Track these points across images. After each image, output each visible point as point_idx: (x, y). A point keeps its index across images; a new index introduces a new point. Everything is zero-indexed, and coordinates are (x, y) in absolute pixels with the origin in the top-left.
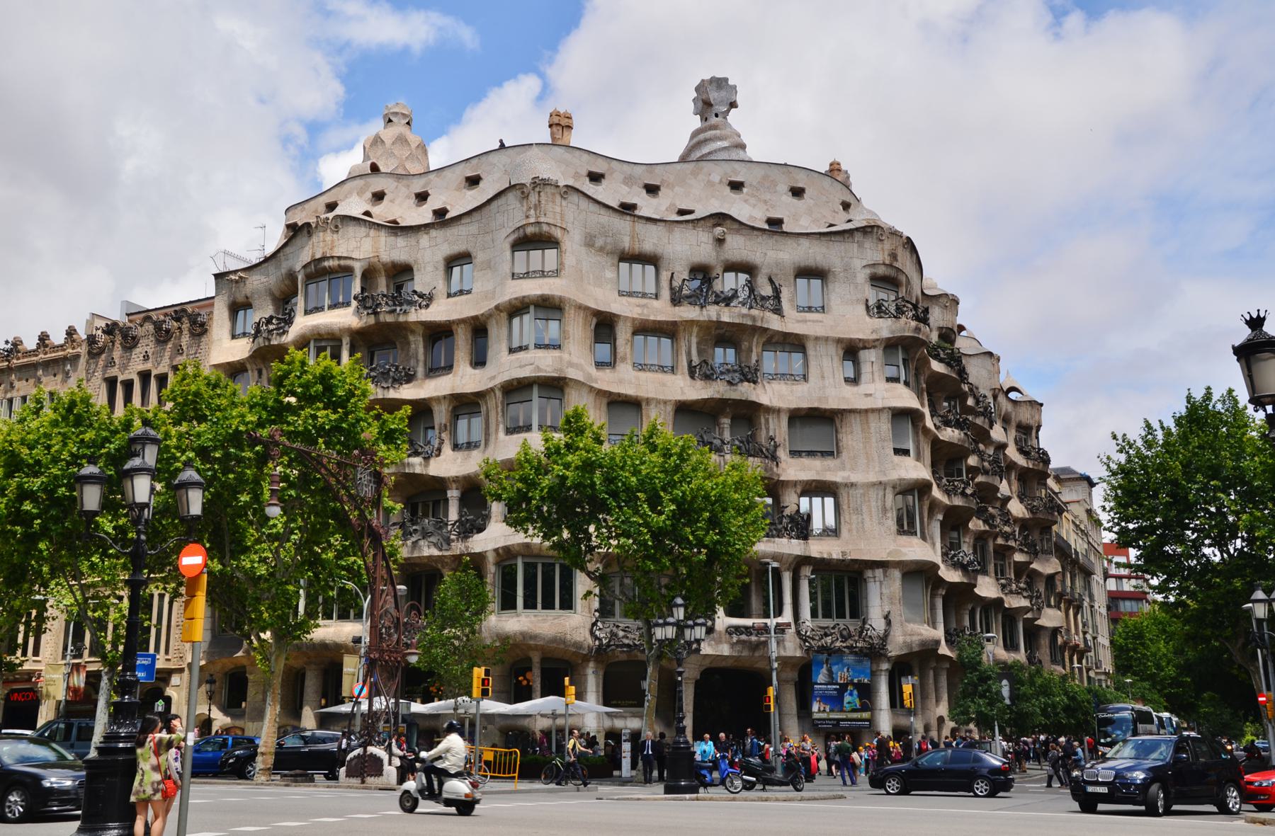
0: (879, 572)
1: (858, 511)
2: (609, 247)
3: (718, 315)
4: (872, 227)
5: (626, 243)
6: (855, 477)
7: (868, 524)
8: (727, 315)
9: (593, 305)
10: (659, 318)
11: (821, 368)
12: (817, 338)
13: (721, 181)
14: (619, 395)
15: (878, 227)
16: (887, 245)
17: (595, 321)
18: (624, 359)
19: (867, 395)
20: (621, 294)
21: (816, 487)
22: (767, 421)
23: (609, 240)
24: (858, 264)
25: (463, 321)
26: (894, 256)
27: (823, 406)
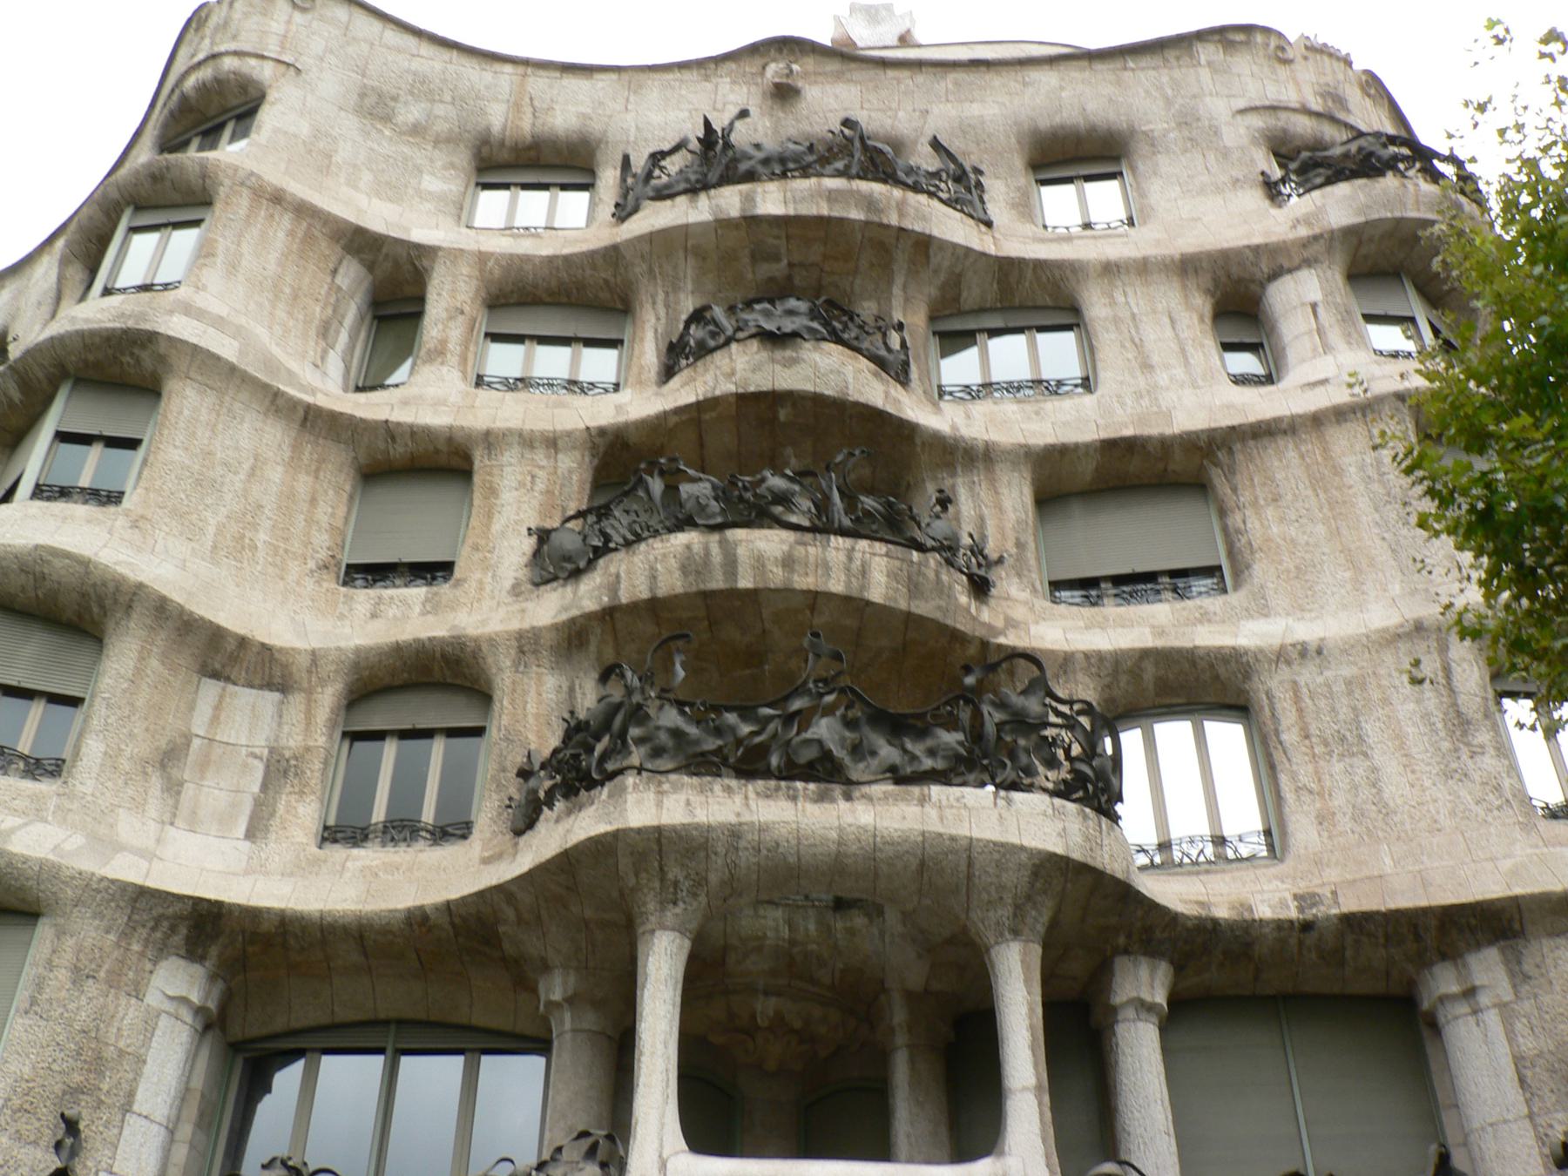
1: (1351, 744)
2: (441, 127)
3: (749, 199)
4: (1248, 29)
5: (496, 118)
6: (1306, 631)
7: (1396, 786)
10: (566, 251)
11: (1139, 346)
12: (1110, 270)
14: (389, 430)
15: (1267, 31)
19: (1313, 385)
21: (1163, 686)
24: (1218, 107)
27: (1154, 429)
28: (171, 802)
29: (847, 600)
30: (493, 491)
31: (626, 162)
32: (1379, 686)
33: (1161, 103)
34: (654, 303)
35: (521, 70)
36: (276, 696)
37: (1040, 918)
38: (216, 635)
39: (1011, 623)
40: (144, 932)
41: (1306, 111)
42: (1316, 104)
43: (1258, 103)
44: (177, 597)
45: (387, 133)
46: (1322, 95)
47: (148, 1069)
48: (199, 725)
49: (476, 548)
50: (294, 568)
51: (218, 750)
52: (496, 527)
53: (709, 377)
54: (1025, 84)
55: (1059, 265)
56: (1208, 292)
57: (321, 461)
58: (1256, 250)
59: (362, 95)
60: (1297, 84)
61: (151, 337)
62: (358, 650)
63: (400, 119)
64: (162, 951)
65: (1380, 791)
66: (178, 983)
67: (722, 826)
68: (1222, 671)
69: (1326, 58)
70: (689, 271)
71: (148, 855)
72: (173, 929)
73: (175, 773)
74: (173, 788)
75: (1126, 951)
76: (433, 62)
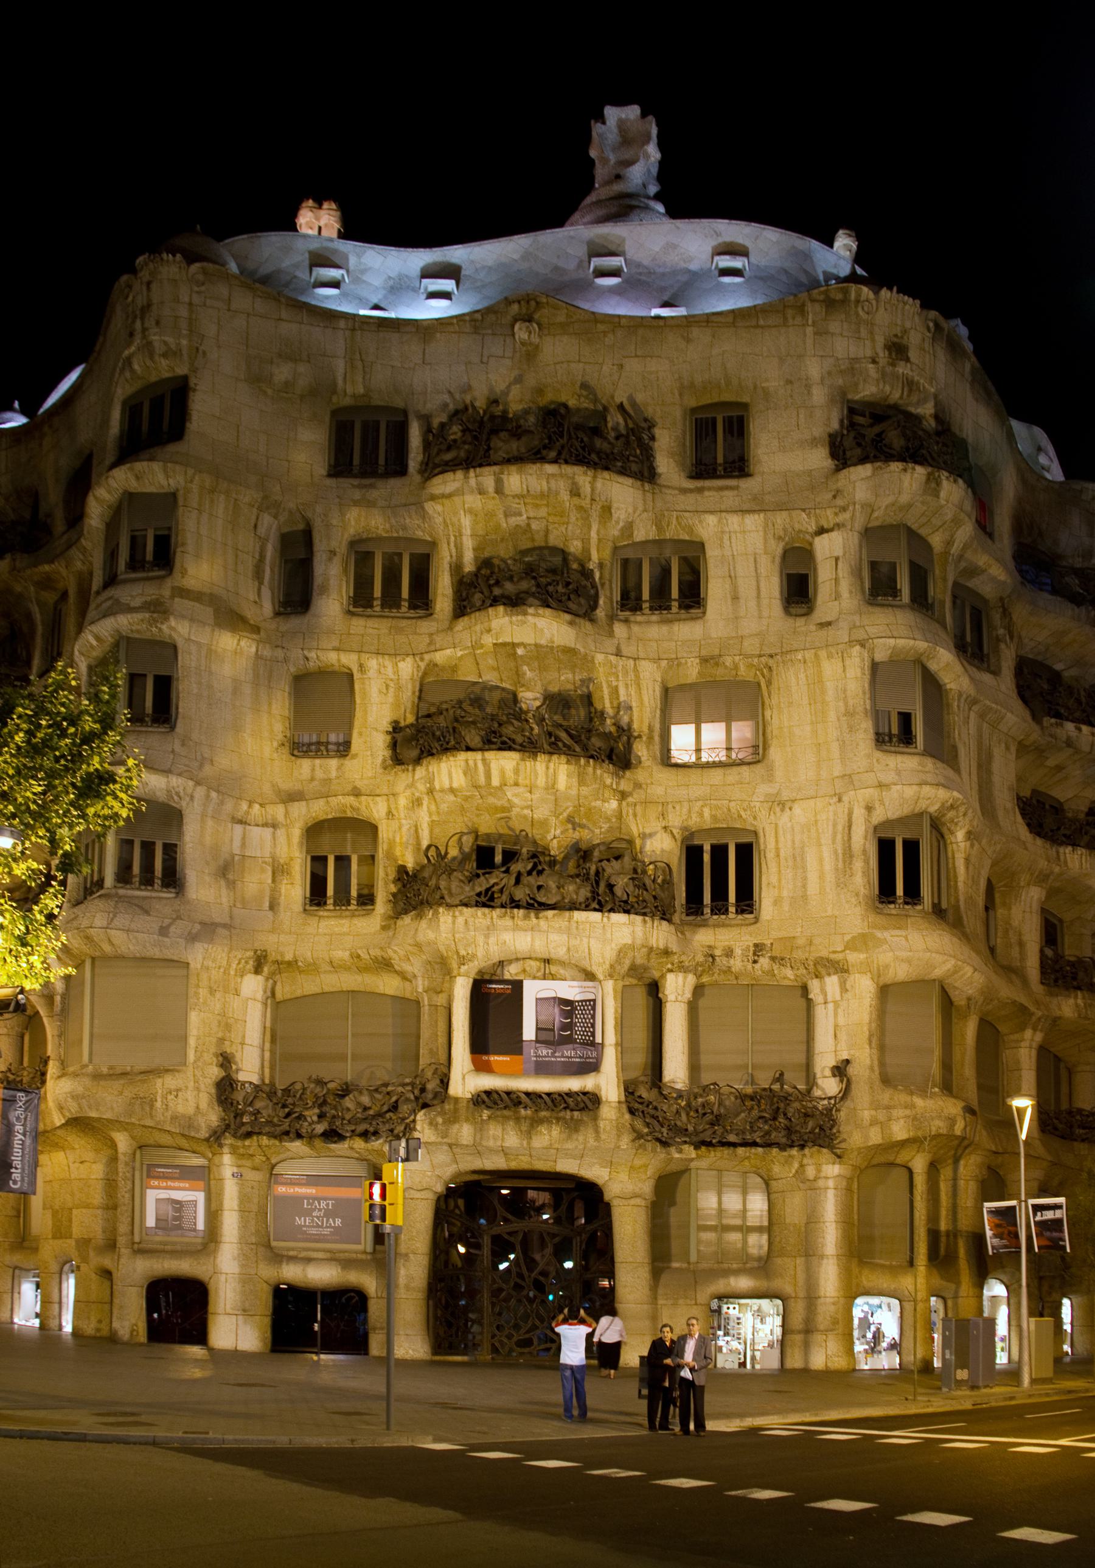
0: (832, 982)
1: (798, 860)
7: (813, 888)
28: (232, 894)
32: (817, 830)
34: (449, 544)
36: (271, 830)
39: (638, 786)
40: (234, 966)
48: (236, 851)
54: (688, 340)
56: (780, 538)
60: (873, 340)
65: (806, 890)
68: (743, 813)
70: (468, 523)
72: (246, 962)
73: (230, 877)
75: (671, 971)
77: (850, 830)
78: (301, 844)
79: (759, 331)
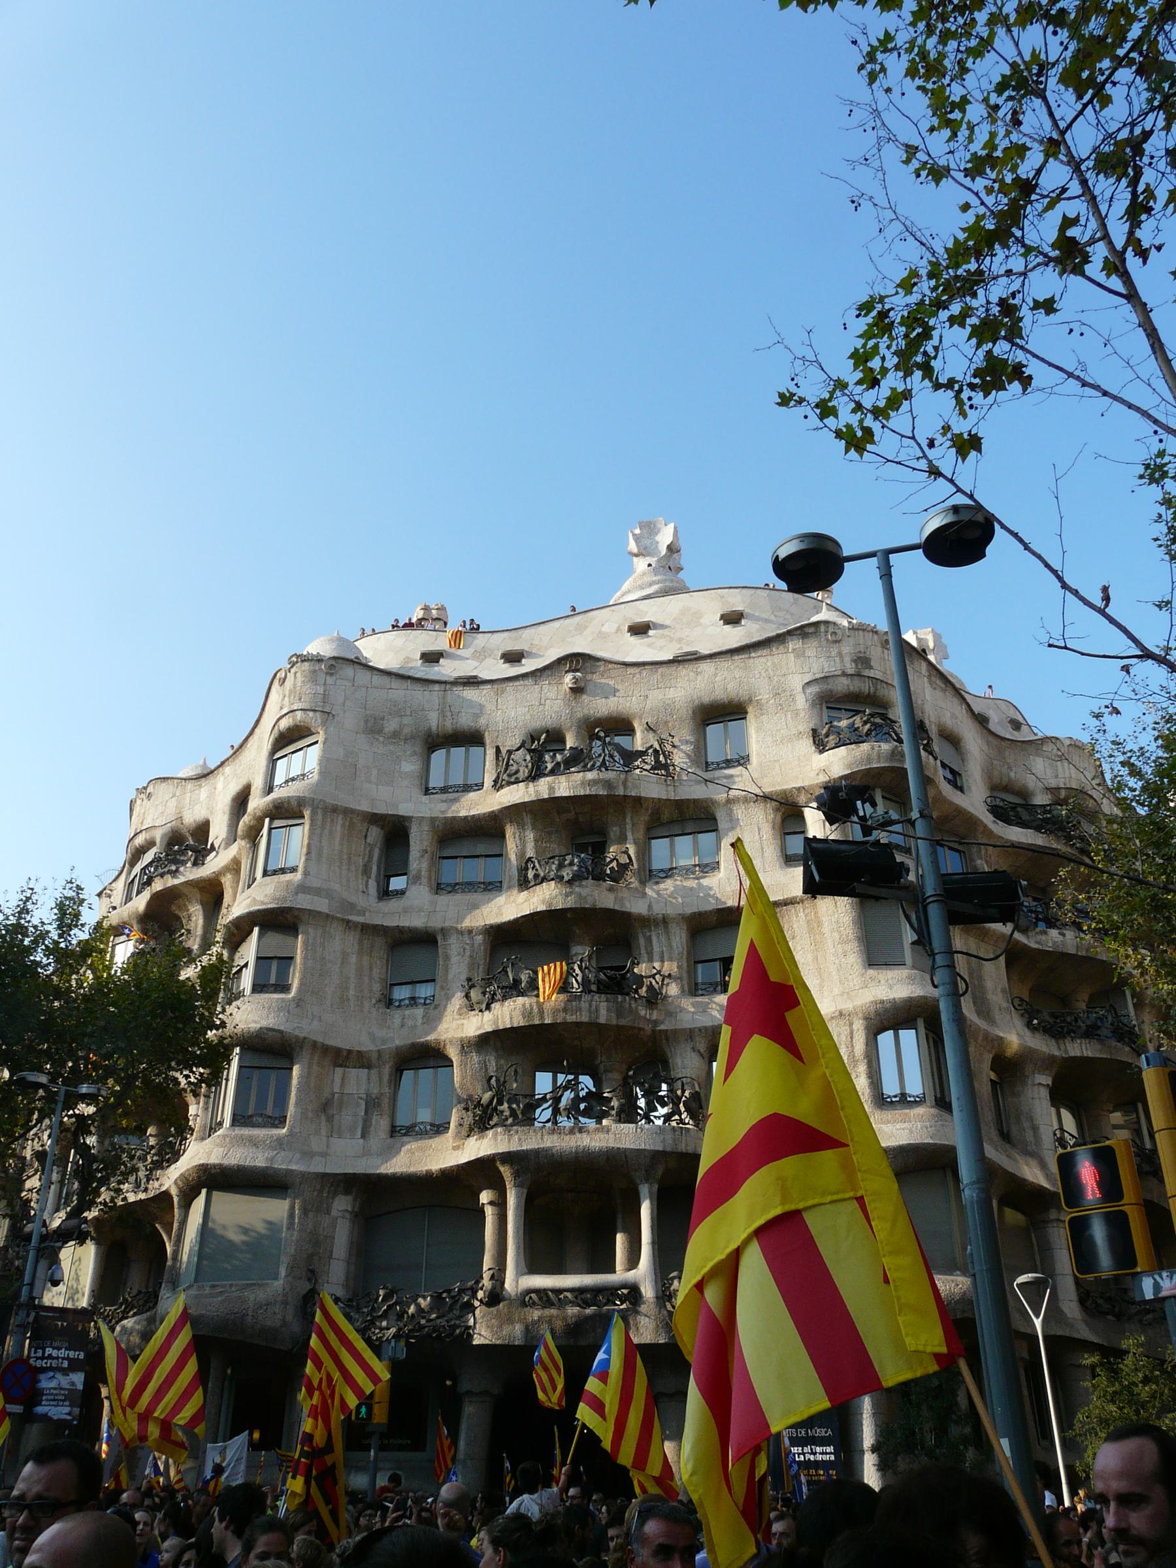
2: (406, 730)
3: (552, 789)
5: (433, 721)
8: (565, 786)
9: (365, 806)
10: (472, 813)
12: (729, 801)
13: (618, 630)
14: (400, 930)
16: (847, 648)
17: (375, 834)
18: (417, 879)
20: (427, 791)
22: (649, 940)
23: (406, 721)
25: (226, 869)
26: (863, 661)
29: (590, 1024)
30: (447, 958)
31: (498, 748)
33: (766, 680)
35: (443, 686)
37: (660, 1171)
38: (338, 1051)
39: (670, 1014)
40: (326, 1190)
41: (844, 674)
42: (850, 668)
43: (818, 676)
44: (319, 1038)
45: (381, 739)
46: (855, 661)
47: (336, 1240)
49: (442, 988)
50: (367, 1004)
51: (345, 1098)
52: (450, 976)
53: (535, 899)
55: (705, 800)
56: (777, 810)
57: (372, 947)
58: (799, 789)
59: (366, 722)
61: (290, 909)
62: (397, 1048)
63: (386, 730)
64: (335, 1194)
66: (342, 1204)
67: (532, 1150)
69: (861, 633)
71: (324, 1155)
73: (330, 1112)
74: (330, 1119)
76: (399, 692)
77: (852, 1038)
78: (390, 1081)
79: (751, 661)
